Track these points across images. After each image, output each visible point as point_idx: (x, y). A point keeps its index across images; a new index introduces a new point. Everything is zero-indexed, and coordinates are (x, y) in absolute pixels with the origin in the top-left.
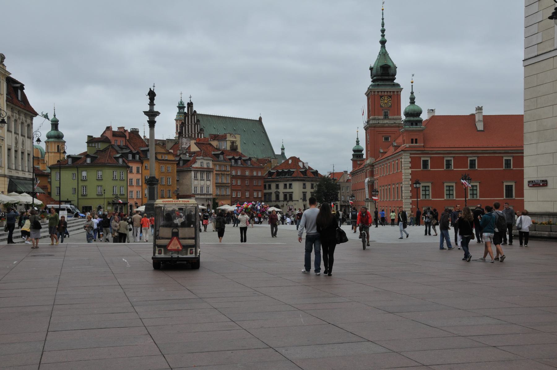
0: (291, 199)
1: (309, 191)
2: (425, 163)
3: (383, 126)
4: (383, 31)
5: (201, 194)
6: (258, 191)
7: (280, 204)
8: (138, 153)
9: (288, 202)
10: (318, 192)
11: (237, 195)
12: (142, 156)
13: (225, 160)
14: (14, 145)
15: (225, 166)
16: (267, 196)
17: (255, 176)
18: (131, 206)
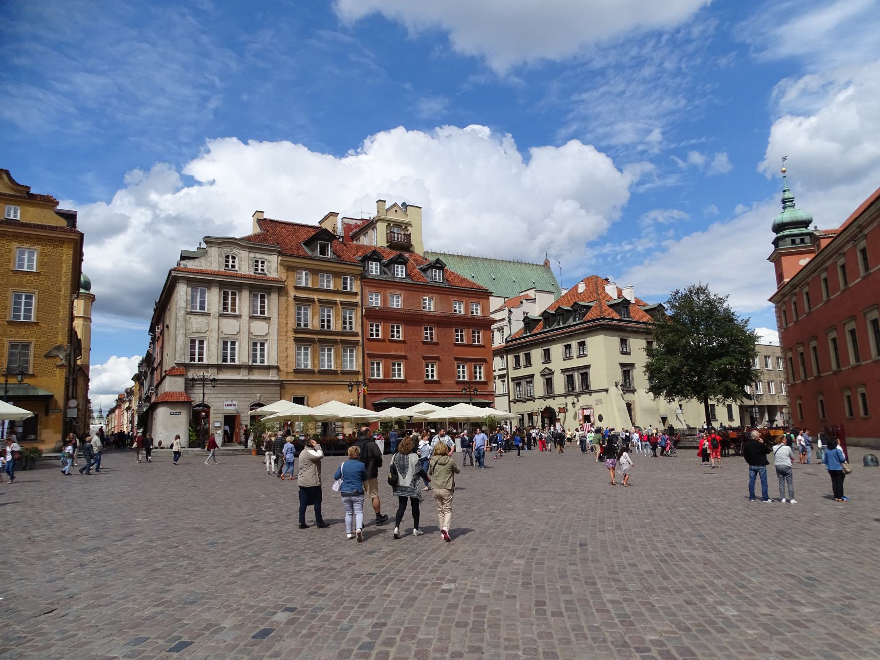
0: (586, 389)
7: (555, 404)
9: (577, 396)
16: (524, 383)
17: (459, 317)
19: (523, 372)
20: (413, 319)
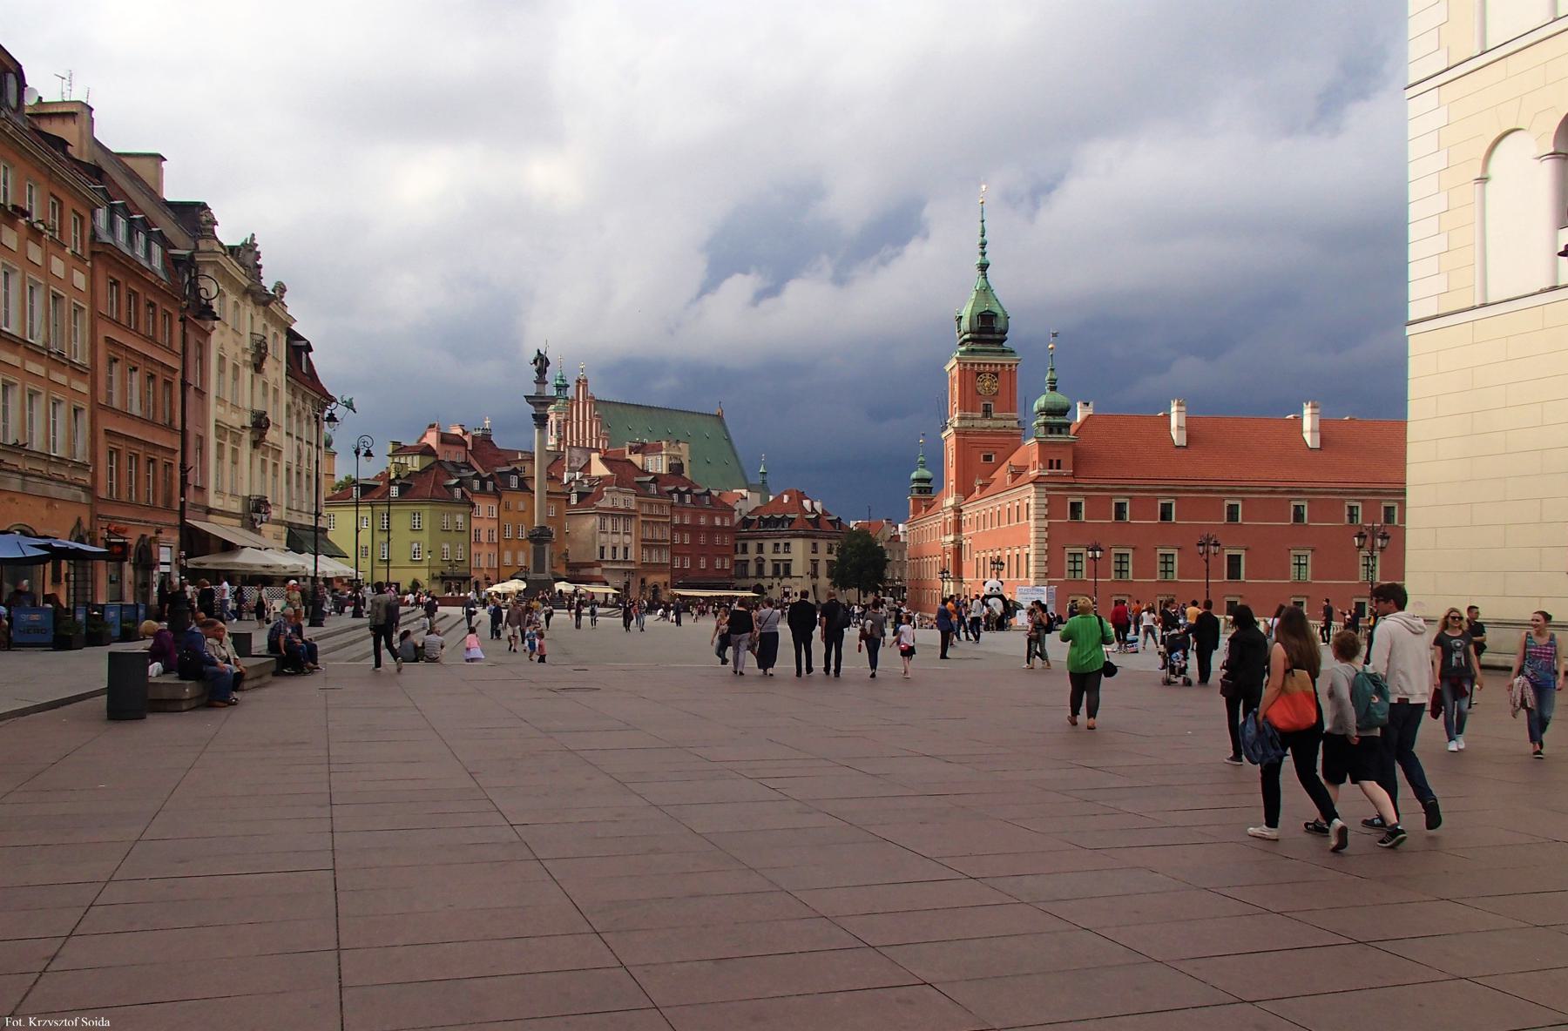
0: (788, 574)
1: (823, 556)
2: (1075, 508)
3: (982, 432)
4: (983, 245)
5: (614, 561)
6: (722, 556)
7: (765, 583)
8: (491, 478)
10: (842, 561)
11: (682, 564)
12: (497, 481)
13: (660, 494)
14: (295, 463)
15: (660, 505)
18: (477, 583)
19: (739, 557)
20: (695, 530)
